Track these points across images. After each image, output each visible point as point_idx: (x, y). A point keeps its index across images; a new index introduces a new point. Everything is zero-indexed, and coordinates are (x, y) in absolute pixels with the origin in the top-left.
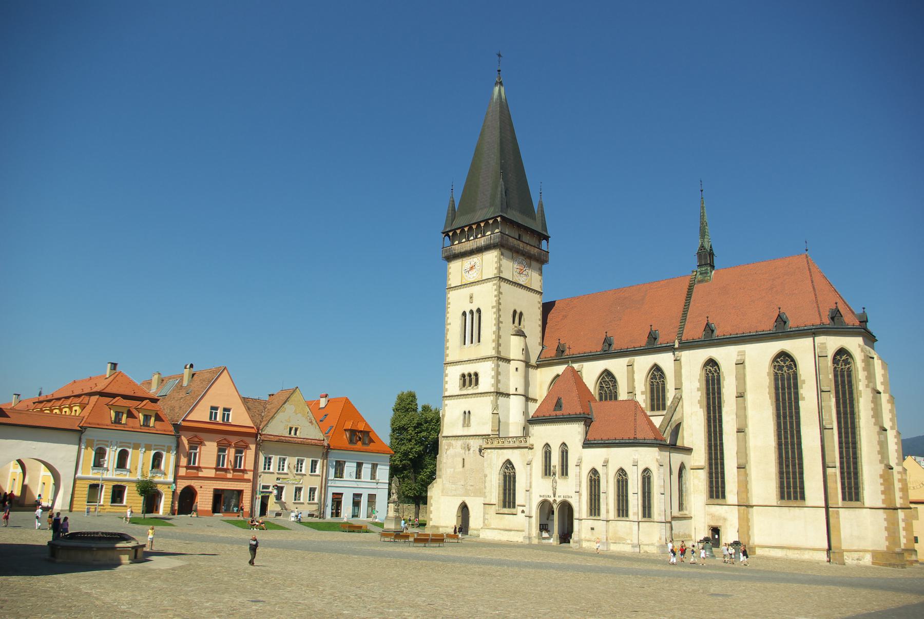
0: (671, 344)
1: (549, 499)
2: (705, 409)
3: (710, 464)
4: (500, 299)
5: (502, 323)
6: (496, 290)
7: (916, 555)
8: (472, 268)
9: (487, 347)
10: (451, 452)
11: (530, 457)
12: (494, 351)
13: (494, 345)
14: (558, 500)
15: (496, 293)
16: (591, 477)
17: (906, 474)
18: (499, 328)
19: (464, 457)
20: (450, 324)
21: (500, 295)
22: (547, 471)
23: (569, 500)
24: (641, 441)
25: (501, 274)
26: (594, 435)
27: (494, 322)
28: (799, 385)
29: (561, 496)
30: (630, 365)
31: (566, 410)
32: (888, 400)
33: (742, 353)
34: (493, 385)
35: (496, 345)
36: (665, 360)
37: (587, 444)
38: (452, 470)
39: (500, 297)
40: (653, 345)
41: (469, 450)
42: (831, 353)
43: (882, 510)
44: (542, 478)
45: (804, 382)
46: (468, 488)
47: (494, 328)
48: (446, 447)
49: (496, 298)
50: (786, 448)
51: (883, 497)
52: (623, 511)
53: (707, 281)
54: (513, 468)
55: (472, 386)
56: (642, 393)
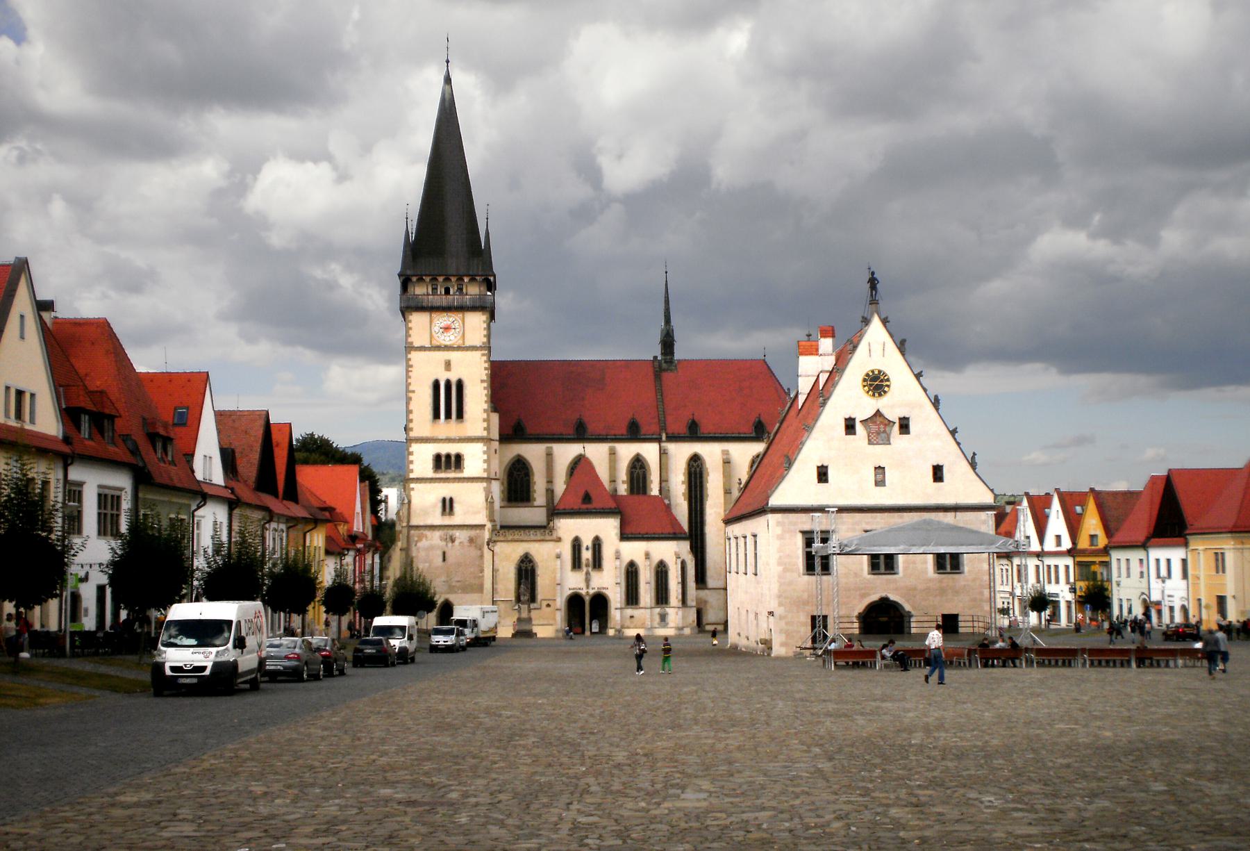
0: (658, 437)
1: (581, 591)
6: (485, 362)
8: (447, 329)
10: (423, 544)
11: (558, 551)
13: (485, 425)
14: (592, 592)
16: (628, 569)
19: (446, 550)
20: (413, 392)
22: (577, 563)
23: (604, 591)
24: (679, 536)
26: (628, 530)
27: (486, 399)
30: (613, 453)
31: (595, 504)
33: (726, 453)
34: (485, 470)
36: (649, 451)
37: (624, 536)
38: (427, 565)
40: (634, 433)
41: (453, 541)
44: (572, 570)
46: (454, 584)
48: (416, 539)
49: (486, 372)
52: (662, 599)
53: (671, 370)
54: (531, 561)
55: (453, 469)
56: (623, 482)
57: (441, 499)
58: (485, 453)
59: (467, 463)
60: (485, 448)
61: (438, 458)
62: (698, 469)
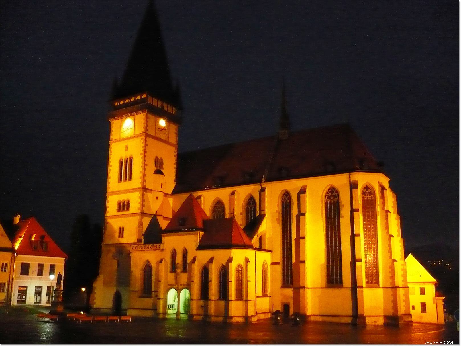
2: (281, 223)
3: (284, 261)
4: (145, 149)
5: (147, 165)
7: (411, 317)
9: (136, 181)
11: (162, 257)
12: (141, 185)
13: (140, 180)
15: (143, 145)
17: (406, 265)
18: (145, 169)
20: (111, 166)
21: (146, 146)
22: (174, 268)
25: (147, 132)
27: (141, 165)
28: (340, 208)
29: (182, 285)
32: (396, 218)
35: (142, 181)
37: (201, 247)
39: (146, 147)
42: (360, 186)
43: (390, 289)
45: (343, 206)
47: (141, 169)
50: (332, 250)
51: (391, 280)
55: (125, 209)
57: (119, 227)
58: (139, 198)
59: (131, 205)
60: (140, 195)
61: (119, 204)
62: (288, 202)
